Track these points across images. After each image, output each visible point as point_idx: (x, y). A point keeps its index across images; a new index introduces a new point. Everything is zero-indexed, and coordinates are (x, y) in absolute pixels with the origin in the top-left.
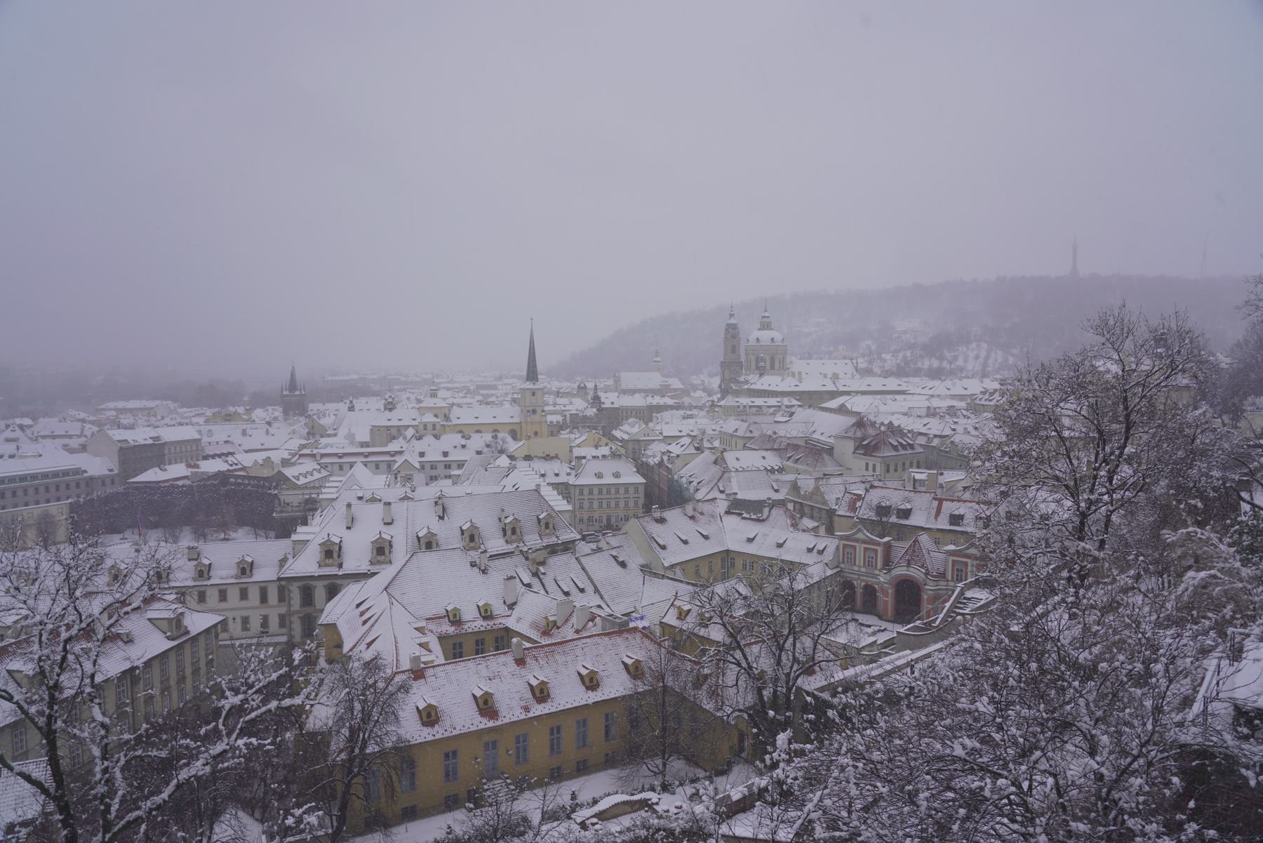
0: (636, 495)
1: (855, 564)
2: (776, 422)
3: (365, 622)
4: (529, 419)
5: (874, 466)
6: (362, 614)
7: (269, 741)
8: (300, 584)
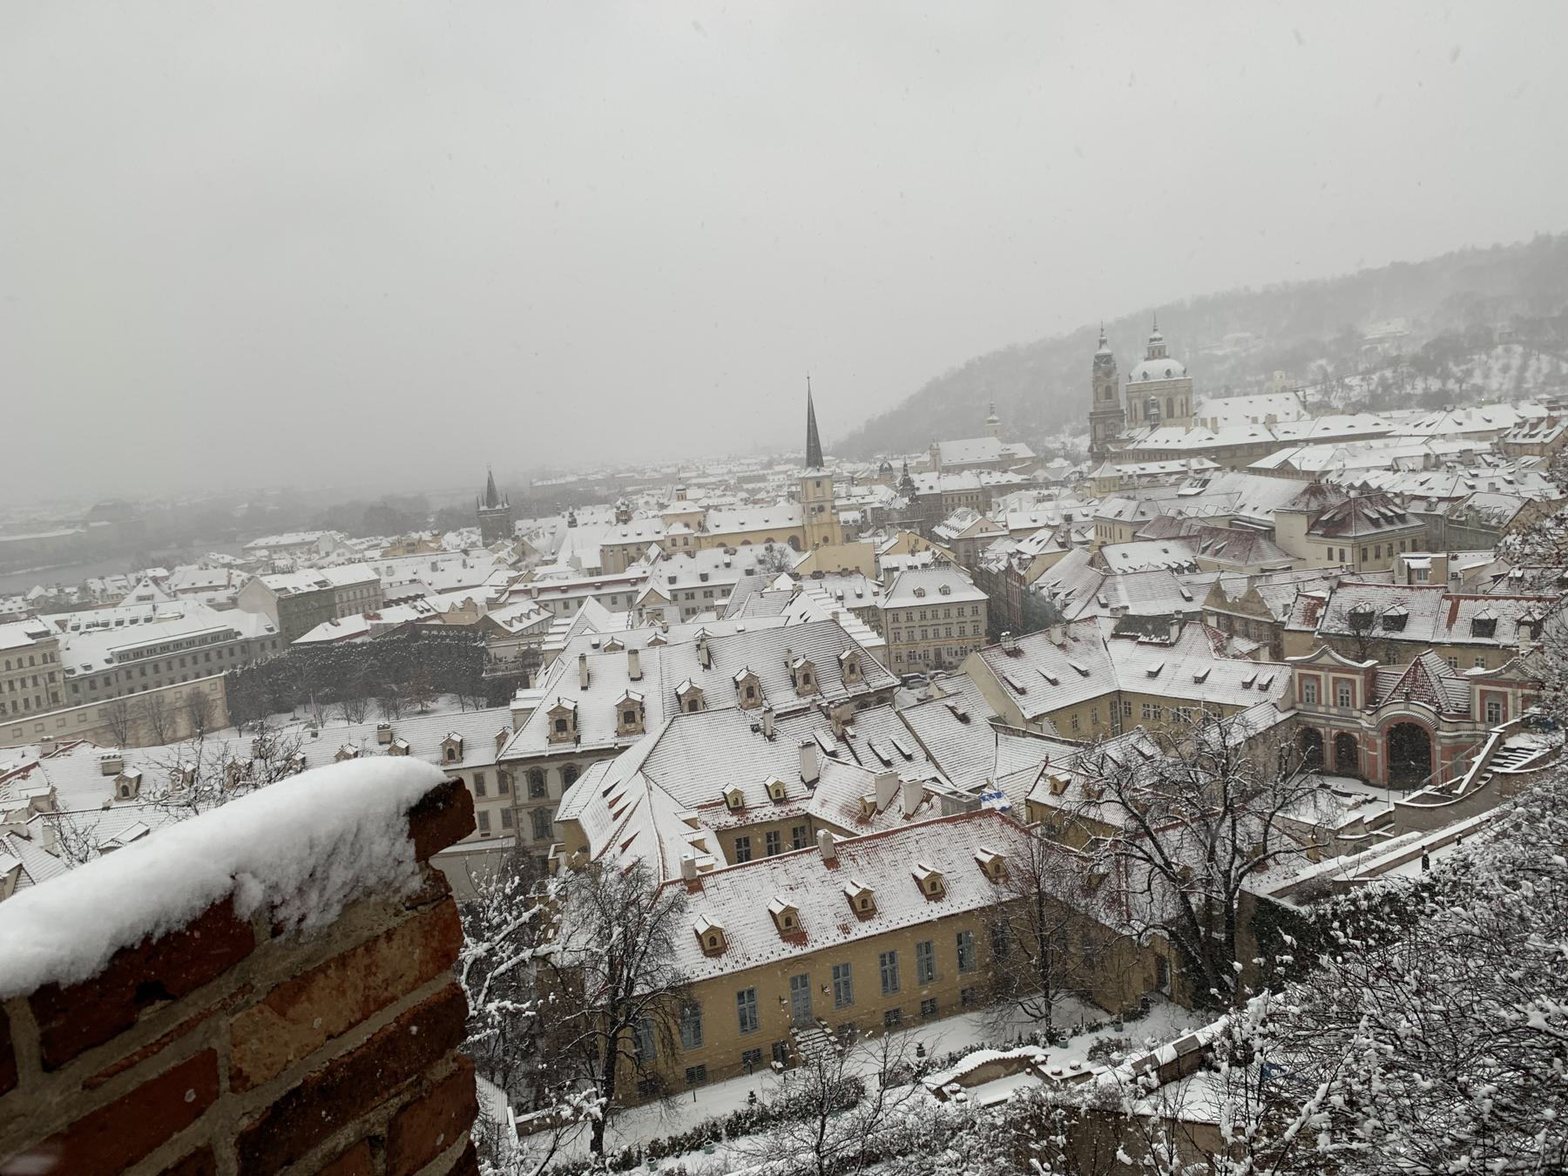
2: (1180, 496)
3: (616, 816)
4: (815, 521)
5: (1342, 553)
6: (612, 805)
7: (528, 1004)
8: (527, 768)
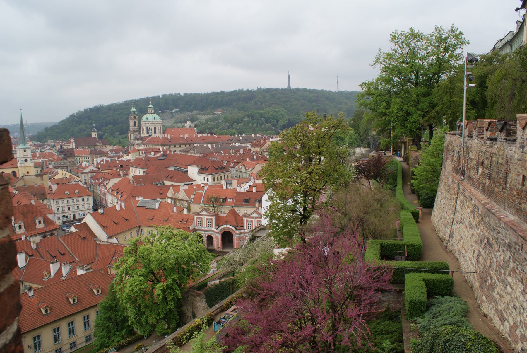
0: (88, 202)
1: (202, 226)
4: (23, 165)
5: (208, 179)
